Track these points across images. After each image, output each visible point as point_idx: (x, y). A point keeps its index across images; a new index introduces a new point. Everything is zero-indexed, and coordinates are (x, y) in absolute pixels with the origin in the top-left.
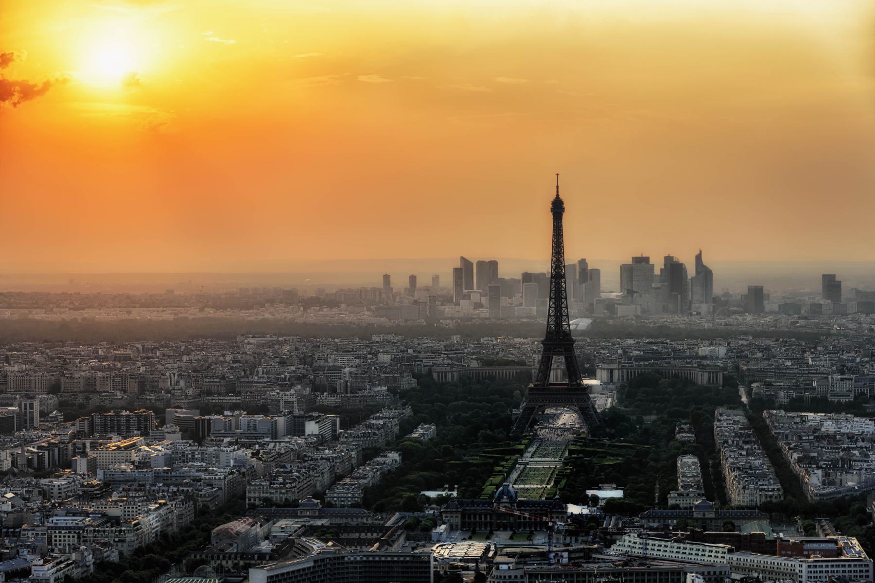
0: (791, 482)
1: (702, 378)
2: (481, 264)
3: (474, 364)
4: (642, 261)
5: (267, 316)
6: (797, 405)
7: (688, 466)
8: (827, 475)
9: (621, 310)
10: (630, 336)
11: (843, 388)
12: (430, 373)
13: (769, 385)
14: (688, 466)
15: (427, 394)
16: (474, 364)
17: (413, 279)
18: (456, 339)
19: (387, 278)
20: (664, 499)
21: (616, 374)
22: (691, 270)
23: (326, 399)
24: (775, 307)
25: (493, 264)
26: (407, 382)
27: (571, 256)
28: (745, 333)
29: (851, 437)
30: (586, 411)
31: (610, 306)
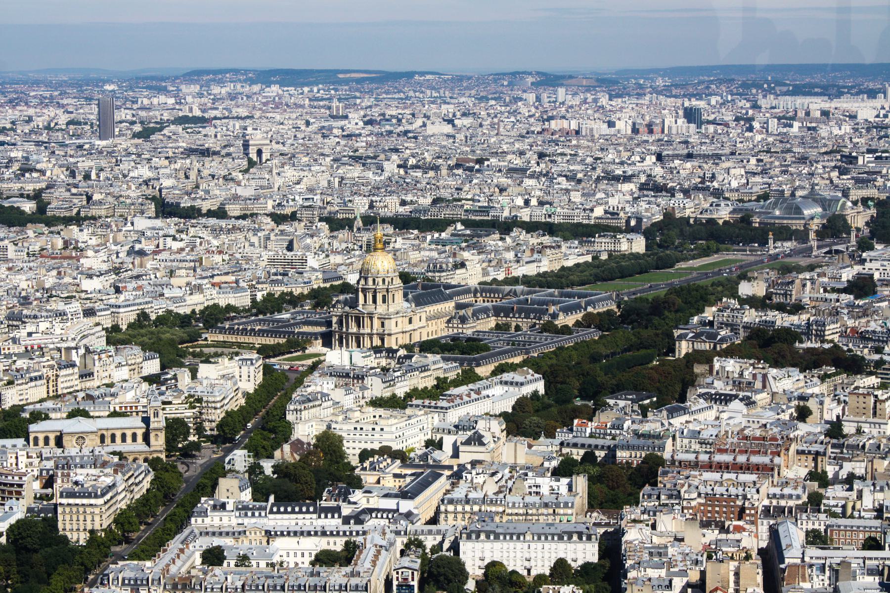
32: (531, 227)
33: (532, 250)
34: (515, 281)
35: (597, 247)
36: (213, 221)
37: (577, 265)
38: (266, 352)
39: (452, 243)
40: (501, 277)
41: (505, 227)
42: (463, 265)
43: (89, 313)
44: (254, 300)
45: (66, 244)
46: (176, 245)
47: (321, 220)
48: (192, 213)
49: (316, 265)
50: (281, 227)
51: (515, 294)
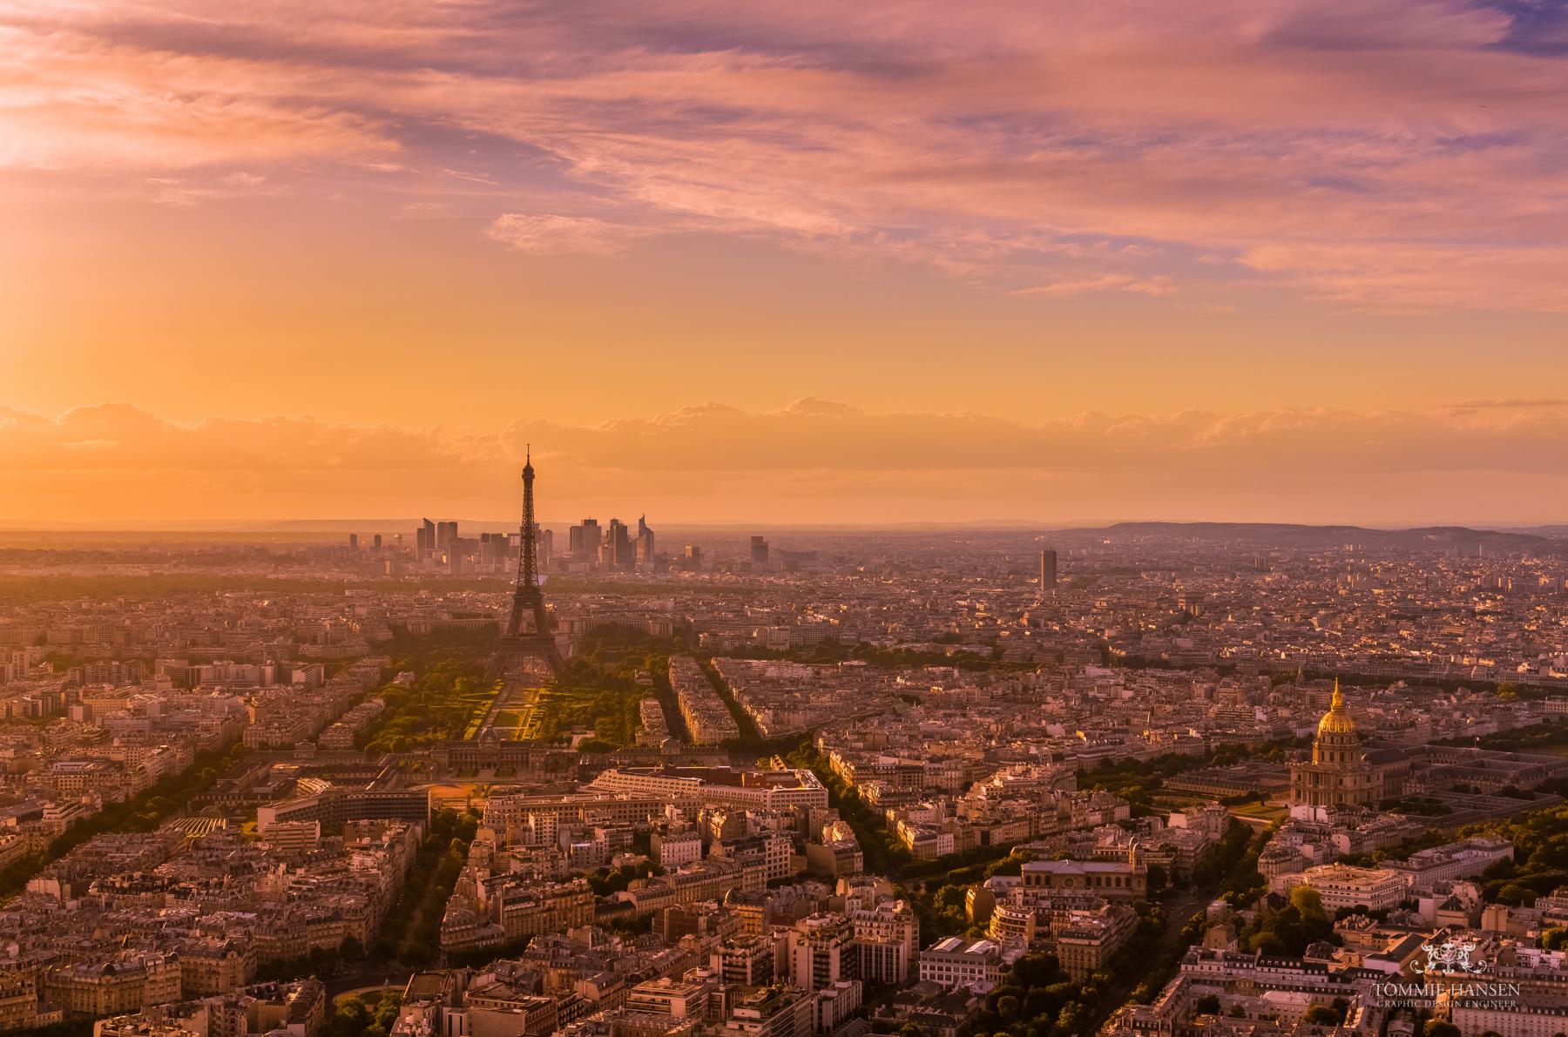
0: (746, 723)
1: (654, 629)
2: (441, 524)
3: (446, 617)
4: (590, 523)
5: (240, 572)
6: (741, 653)
7: (649, 707)
8: (776, 715)
9: (572, 567)
10: (586, 591)
11: (779, 635)
12: (405, 626)
13: (714, 635)
14: (649, 707)
15: (401, 642)
16: (446, 617)
17: (378, 538)
18: (423, 594)
19: (353, 537)
20: (633, 739)
21: (576, 625)
22: (633, 531)
23: (308, 649)
24: (710, 565)
25: (454, 525)
26: (385, 635)
27: (539, 518)
28: (687, 589)
29: (793, 682)
30: (553, 661)
31: (562, 564)
32: (1476, 687)
33: (1481, 711)
34: (1469, 741)
35: (1547, 710)
36: (1159, 673)
37: (1528, 728)
38: (1226, 802)
39: (1395, 700)
40: (1451, 736)
41: (1448, 686)
42: (1412, 724)
43: (1058, 758)
44: (1208, 751)
45: (1025, 689)
46: (1127, 694)
47: (1262, 673)
48: (1135, 663)
49: (1264, 718)
50: (1226, 680)
51: (1471, 755)
